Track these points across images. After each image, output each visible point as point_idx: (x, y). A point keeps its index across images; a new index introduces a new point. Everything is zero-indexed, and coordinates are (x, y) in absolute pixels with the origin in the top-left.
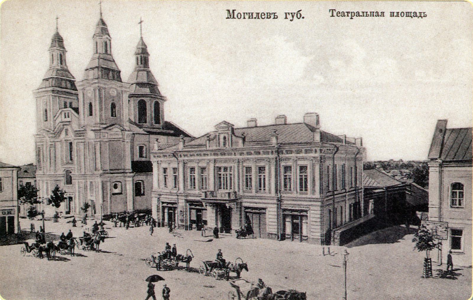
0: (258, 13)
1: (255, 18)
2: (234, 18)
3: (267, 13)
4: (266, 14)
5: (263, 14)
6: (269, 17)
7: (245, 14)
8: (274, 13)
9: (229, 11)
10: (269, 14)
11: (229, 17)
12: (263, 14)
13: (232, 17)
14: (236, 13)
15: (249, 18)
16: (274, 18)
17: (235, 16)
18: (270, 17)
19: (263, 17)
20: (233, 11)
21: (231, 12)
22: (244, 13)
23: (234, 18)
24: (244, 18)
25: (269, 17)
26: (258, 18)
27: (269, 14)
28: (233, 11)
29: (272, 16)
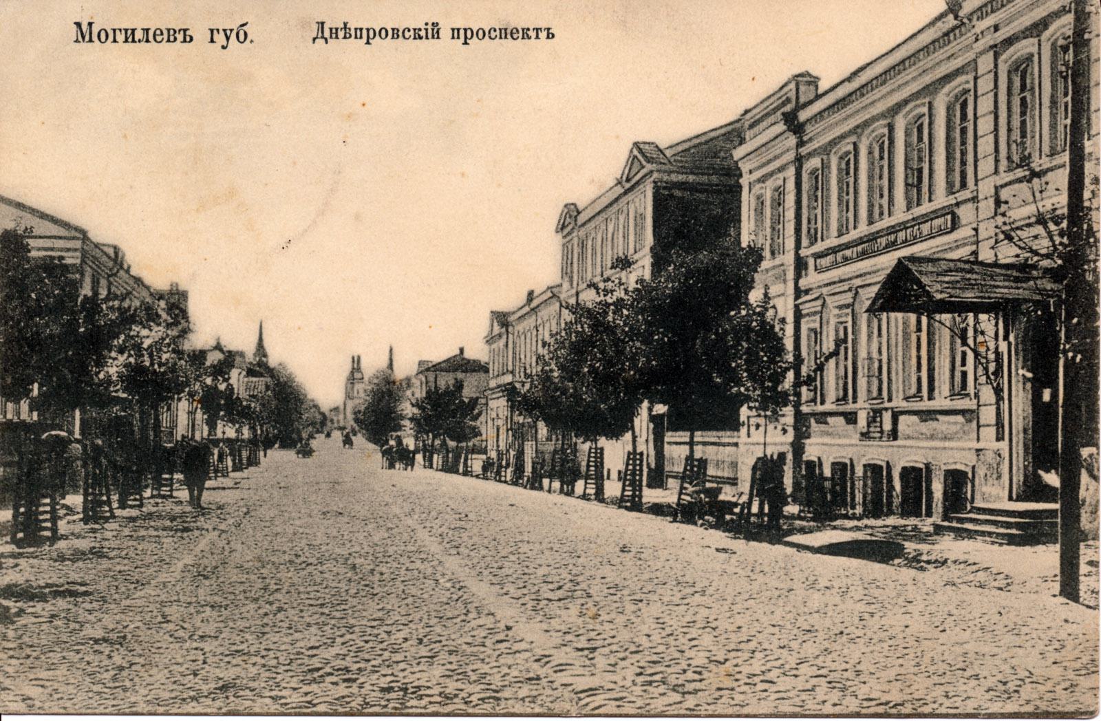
0: (147, 30)
1: (140, 41)
2: (91, 40)
3: (169, 30)
4: (165, 33)
5: (158, 32)
6: (172, 38)
7: (118, 32)
8: (185, 30)
9: (78, 25)
10: (172, 32)
11: (80, 39)
12: (158, 32)
13: (87, 38)
14: (95, 30)
15: (126, 41)
16: (185, 41)
17: (95, 38)
18: (175, 39)
19: (159, 39)
20: (90, 24)
21: (85, 27)
22: (114, 30)
23: (91, 40)
24: (115, 41)
25: (172, 38)
26: (147, 41)
27: (172, 32)
28: (90, 24)
29: (180, 37)
